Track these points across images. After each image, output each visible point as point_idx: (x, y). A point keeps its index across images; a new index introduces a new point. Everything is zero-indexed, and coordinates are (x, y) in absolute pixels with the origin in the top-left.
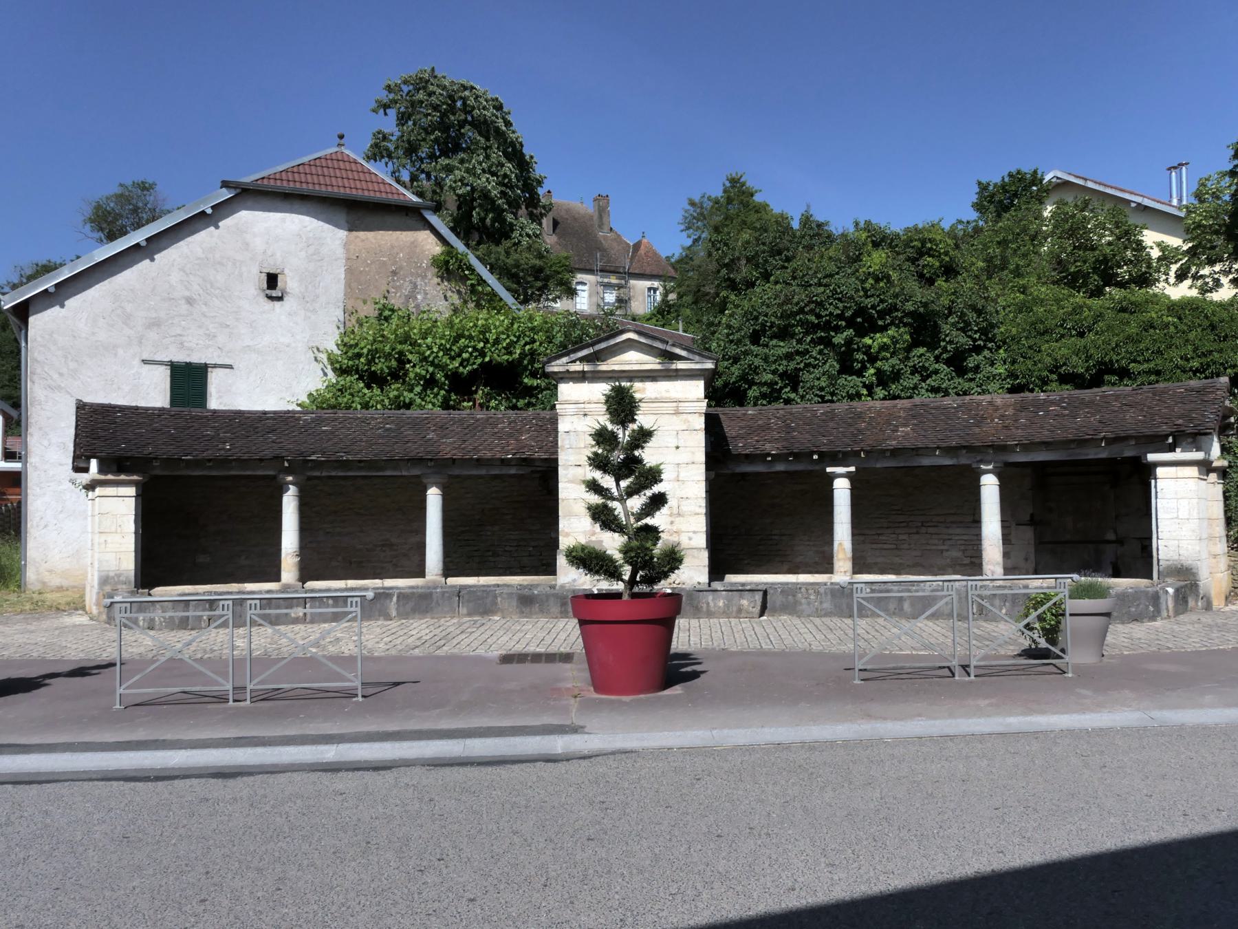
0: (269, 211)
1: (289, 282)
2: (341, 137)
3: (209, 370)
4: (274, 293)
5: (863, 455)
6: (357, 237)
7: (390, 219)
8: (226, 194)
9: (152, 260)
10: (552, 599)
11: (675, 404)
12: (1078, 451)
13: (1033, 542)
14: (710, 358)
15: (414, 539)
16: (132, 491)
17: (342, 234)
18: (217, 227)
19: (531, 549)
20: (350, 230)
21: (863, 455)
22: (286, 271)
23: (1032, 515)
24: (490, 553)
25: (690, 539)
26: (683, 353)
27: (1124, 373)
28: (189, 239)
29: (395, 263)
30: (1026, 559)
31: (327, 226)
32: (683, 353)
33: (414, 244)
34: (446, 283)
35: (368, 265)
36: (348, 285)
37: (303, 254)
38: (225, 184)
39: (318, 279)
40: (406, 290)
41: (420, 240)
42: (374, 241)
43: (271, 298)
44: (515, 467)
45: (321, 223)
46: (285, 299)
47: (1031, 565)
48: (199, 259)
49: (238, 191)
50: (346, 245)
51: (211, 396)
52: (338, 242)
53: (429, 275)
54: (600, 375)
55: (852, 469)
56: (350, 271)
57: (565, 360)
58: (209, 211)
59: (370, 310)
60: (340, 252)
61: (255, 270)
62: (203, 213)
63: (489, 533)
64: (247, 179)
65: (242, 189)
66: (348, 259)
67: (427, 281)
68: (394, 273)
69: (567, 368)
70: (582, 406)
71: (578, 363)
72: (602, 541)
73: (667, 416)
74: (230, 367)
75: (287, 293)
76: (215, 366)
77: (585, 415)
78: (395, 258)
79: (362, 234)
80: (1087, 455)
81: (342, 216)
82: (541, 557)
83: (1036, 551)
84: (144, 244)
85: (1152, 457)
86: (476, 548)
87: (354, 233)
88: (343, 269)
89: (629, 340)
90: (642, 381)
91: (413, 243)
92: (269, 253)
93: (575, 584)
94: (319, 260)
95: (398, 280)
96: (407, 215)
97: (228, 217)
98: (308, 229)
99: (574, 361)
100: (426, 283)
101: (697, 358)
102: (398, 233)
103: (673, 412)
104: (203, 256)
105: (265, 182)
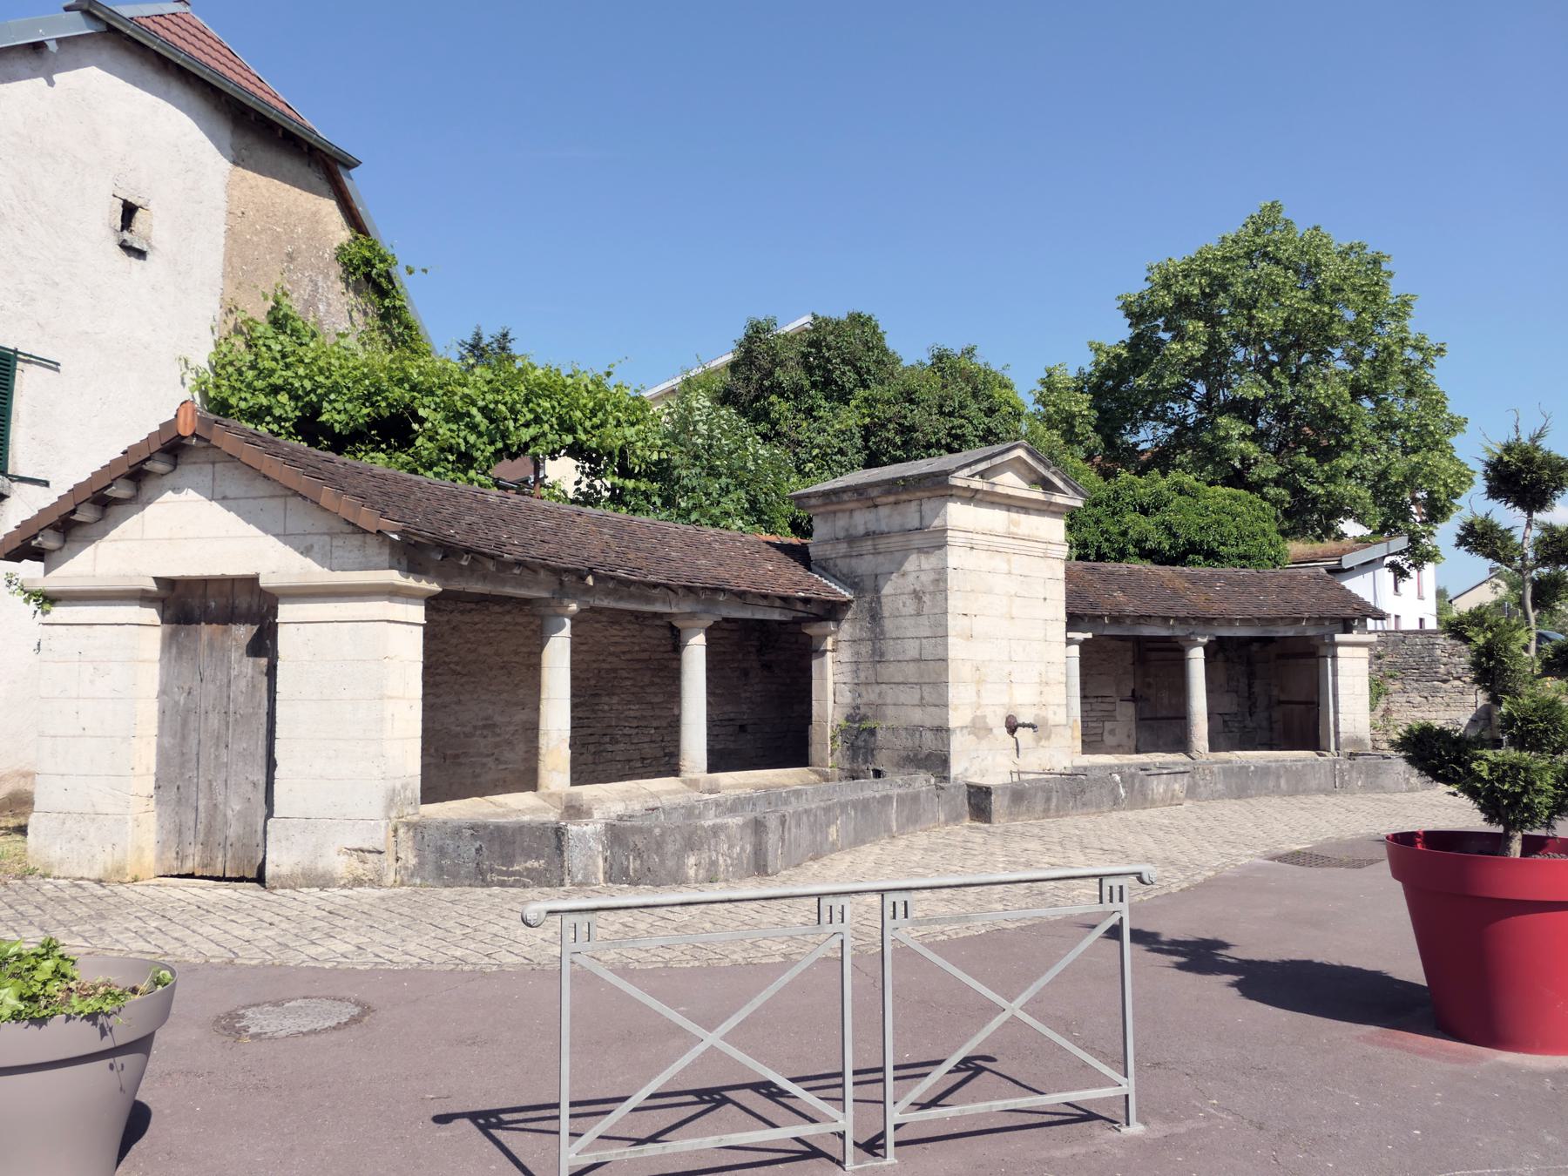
3: (20, 365)
5: (1106, 621)
6: (243, 179)
7: (289, 164)
10: (1040, 794)
11: (1044, 546)
12: (1270, 628)
13: (1133, 718)
14: (1082, 495)
15: (521, 716)
19: (653, 731)
20: (235, 163)
21: (1106, 621)
23: (1133, 691)
24: (607, 739)
25: (1055, 714)
26: (1060, 484)
27: (1211, 555)
29: (291, 241)
30: (1129, 736)
32: (1060, 484)
33: (315, 217)
34: (351, 295)
35: (257, 233)
36: (228, 259)
40: (305, 290)
41: (323, 213)
44: (778, 611)
47: (1132, 743)
51: (17, 420)
55: (1089, 635)
56: (231, 233)
57: (966, 472)
59: (258, 310)
63: (606, 707)
67: (329, 284)
68: (290, 257)
69: (968, 483)
70: (975, 536)
71: (977, 477)
72: (985, 717)
73: (1037, 559)
74: (54, 366)
76: (31, 359)
77: (972, 548)
80: (1277, 632)
82: (663, 744)
83: (1137, 727)
85: (1339, 637)
86: (590, 731)
89: (1019, 458)
90: (1018, 512)
91: (314, 214)
93: (968, 774)
96: (309, 166)
99: (973, 476)
101: (1070, 492)
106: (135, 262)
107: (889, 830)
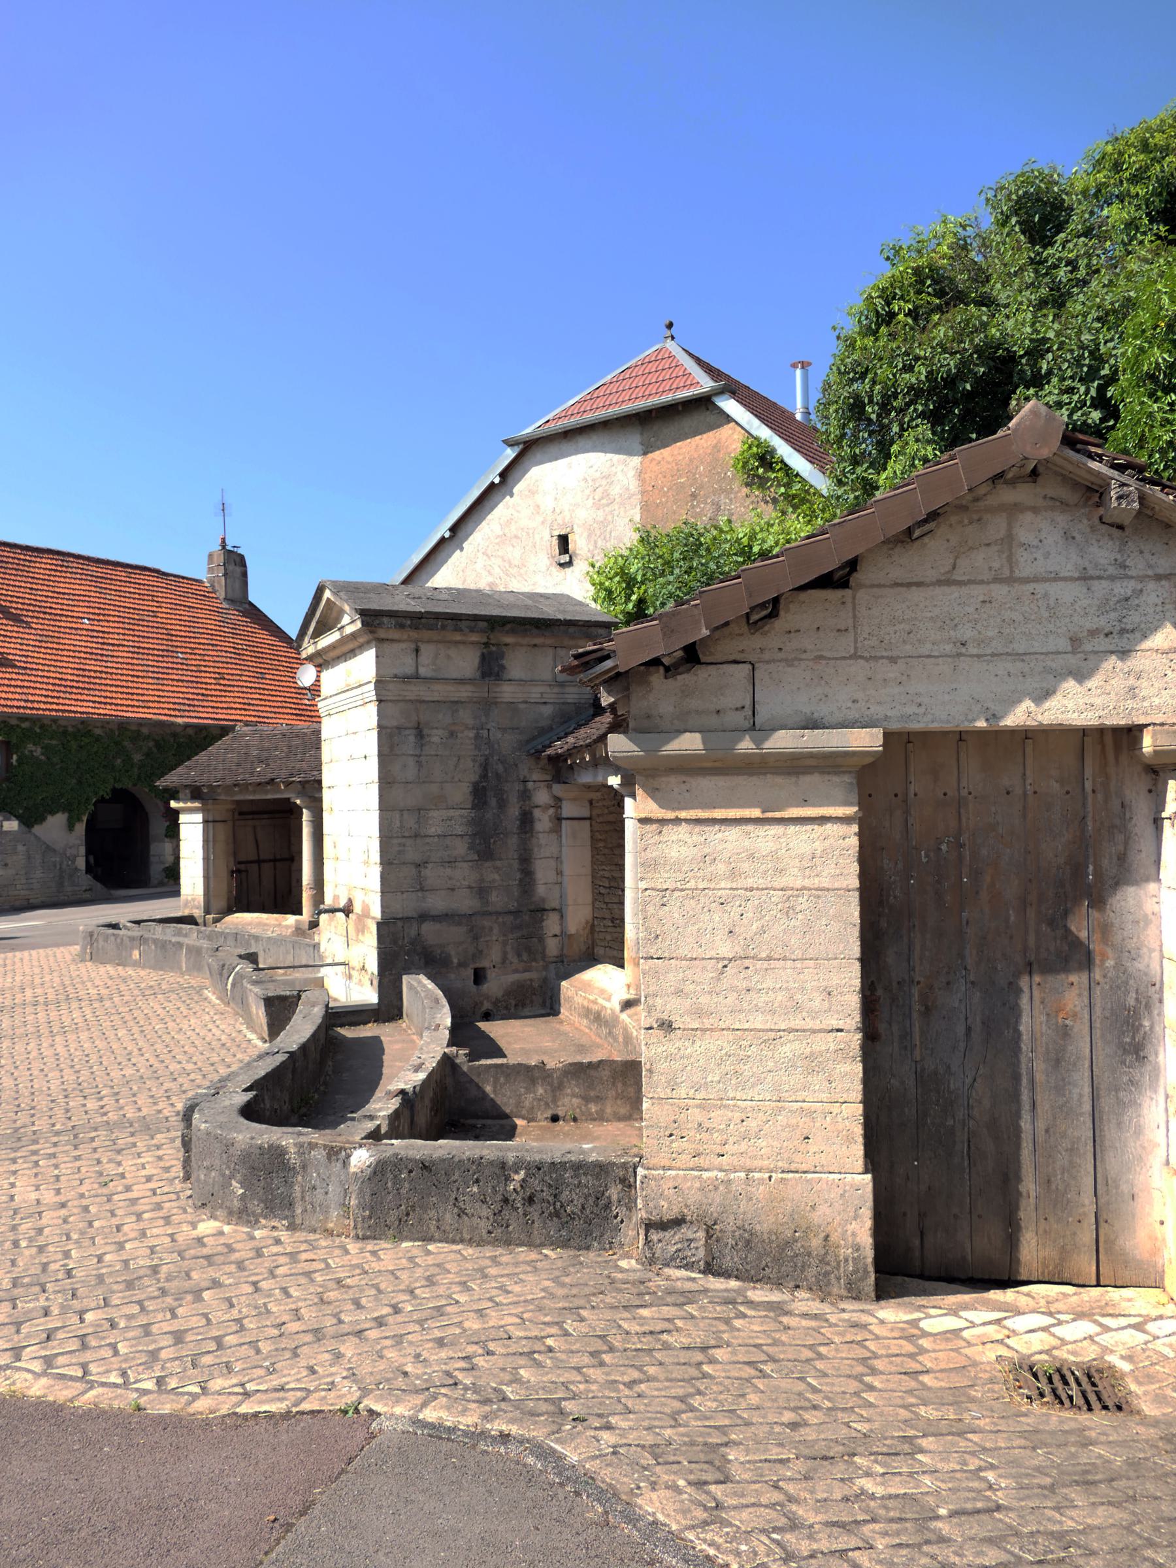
0: (556, 459)
1: (578, 543)
2: (670, 326)
4: (566, 558)
7: (688, 422)
8: (510, 454)
9: (462, 549)
16: (199, 817)
17: (636, 461)
18: (512, 495)
22: (575, 527)
28: (489, 517)
31: (616, 458)
37: (591, 501)
38: (510, 443)
39: (608, 529)
41: (724, 440)
42: (670, 459)
43: (561, 565)
45: (609, 456)
46: (575, 563)
48: (498, 536)
49: (521, 446)
50: (640, 474)
52: (631, 473)
53: (736, 486)
54: (332, 654)
58: (497, 480)
60: (634, 486)
61: (547, 536)
62: (492, 484)
64: (528, 431)
65: (525, 443)
66: (643, 493)
68: (694, 496)
75: (576, 555)
78: (694, 475)
79: (657, 455)
81: (634, 438)
84: (447, 535)
87: (650, 456)
88: (639, 507)
91: (715, 446)
92: (558, 511)
94: (608, 505)
95: (698, 505)
97: (519, 480)
98: (595, 468)
100: (731, 500)
102: (698, 438)
103: (361, 702)
104: (501, 533)
105: (552, 425)
106: (568, 570)
107: (180, 968)
